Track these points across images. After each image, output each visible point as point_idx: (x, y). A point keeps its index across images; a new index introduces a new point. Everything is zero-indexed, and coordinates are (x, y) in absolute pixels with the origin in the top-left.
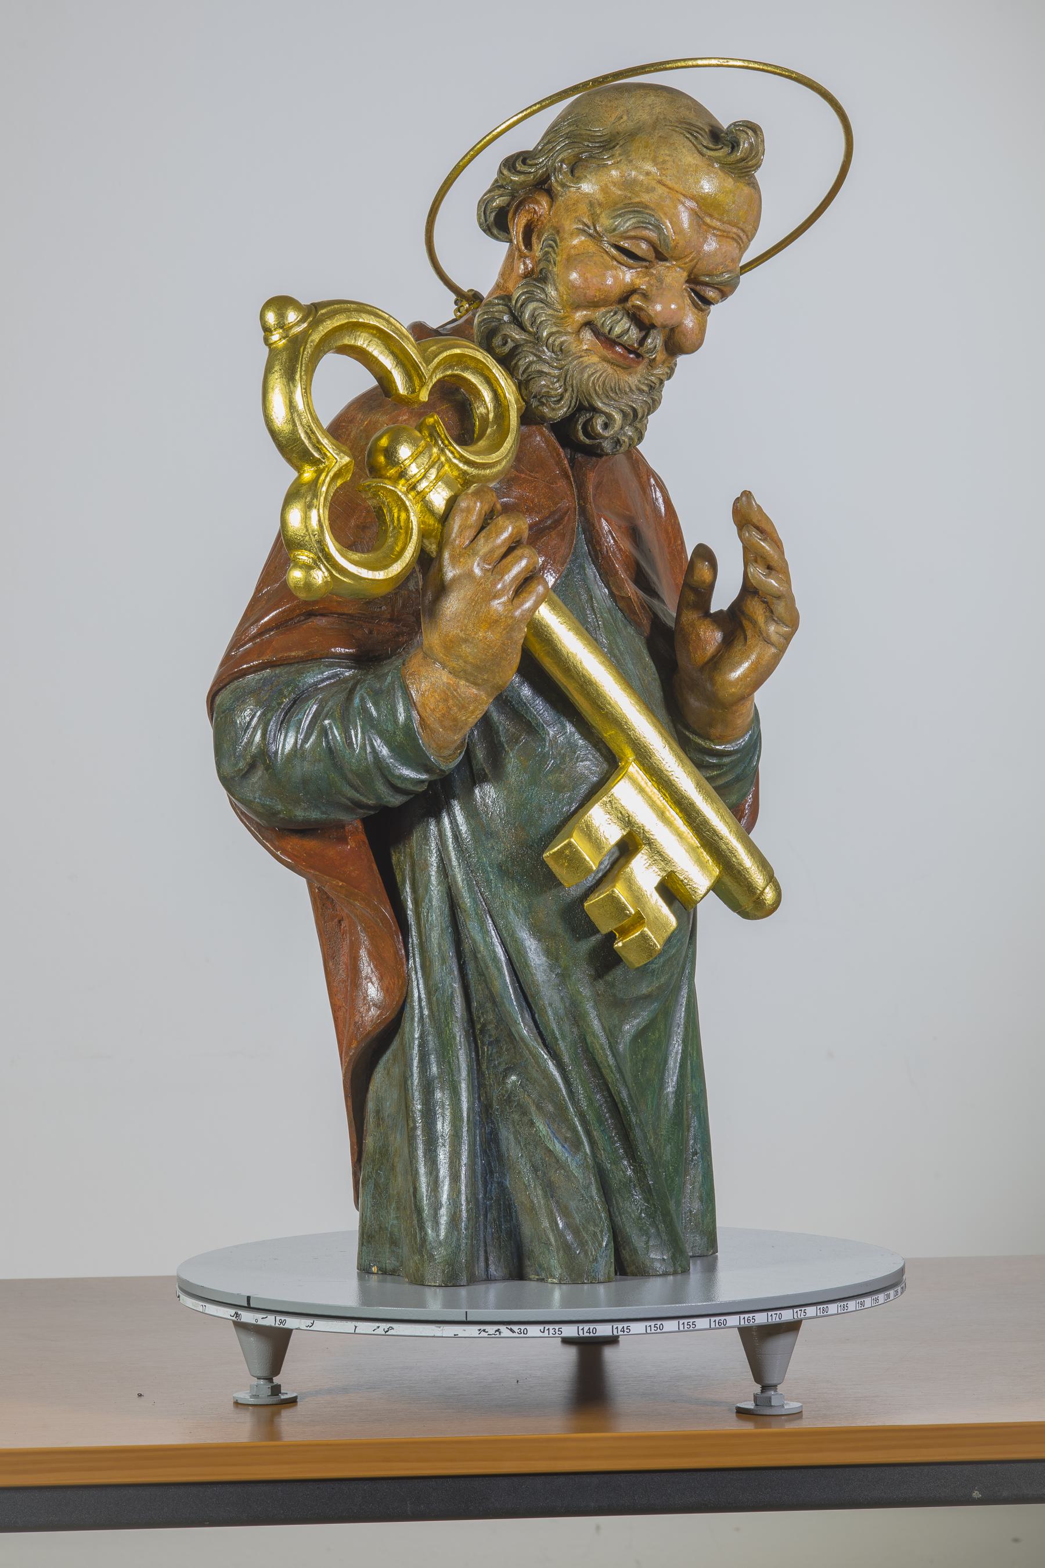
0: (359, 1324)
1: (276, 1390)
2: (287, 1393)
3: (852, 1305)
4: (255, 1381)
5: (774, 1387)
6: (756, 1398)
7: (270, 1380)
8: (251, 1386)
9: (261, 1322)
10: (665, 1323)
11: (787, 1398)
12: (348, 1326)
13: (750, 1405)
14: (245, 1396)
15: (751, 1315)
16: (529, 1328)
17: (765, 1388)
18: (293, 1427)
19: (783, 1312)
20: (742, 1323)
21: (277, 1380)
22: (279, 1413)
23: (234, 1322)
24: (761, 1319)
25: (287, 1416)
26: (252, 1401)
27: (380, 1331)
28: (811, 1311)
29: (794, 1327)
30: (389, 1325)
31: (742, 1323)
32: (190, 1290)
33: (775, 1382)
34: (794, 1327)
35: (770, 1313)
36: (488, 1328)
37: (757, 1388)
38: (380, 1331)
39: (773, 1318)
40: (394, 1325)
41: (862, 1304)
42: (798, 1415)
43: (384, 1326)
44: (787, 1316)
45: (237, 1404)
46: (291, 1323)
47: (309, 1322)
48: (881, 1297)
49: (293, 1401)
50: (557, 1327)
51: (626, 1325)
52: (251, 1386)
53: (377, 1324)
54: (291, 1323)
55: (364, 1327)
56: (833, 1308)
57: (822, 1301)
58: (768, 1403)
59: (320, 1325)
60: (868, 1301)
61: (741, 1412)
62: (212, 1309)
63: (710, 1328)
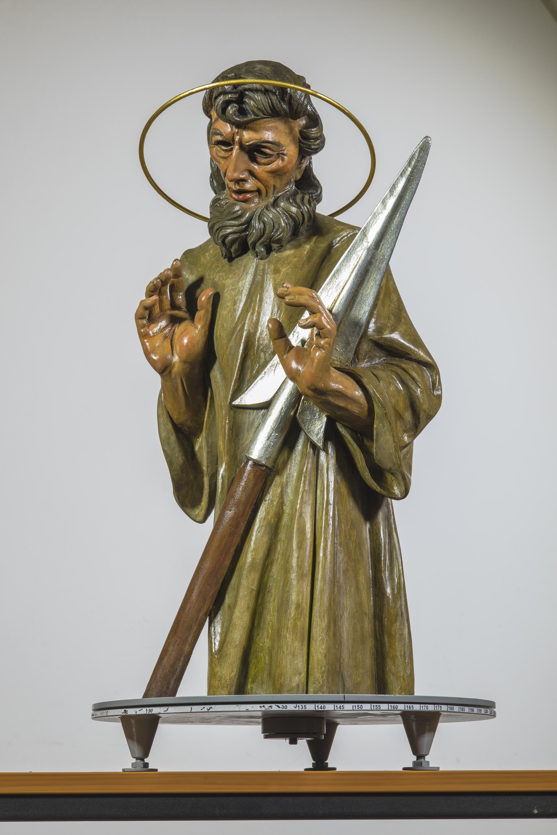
0: (193, 707)
9: (139, 713)
12: (187, 709)
15: (411, 705)
20: (406, 708)
24: (417, 707)
27: (205, 710)
31: (406, 708)
35: (421, 705)
36: (266, 705)
39: (423, 708)
40: (213, 706)
43: (207, 707)
44: (431, 708)
46: (156, 710)
47: (165, 708)
53: (202, 706)
54: (156, 710)
55: (196, 708)
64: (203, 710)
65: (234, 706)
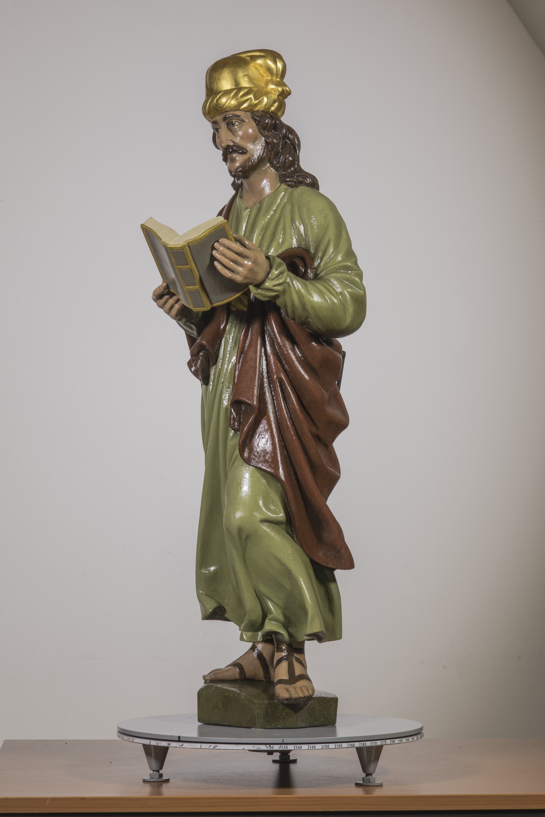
0: (203, 745)
1: (161, 776)
2: (165, 778)
3: (404, 740)
4: (152, 772)
5: (371, 774)
6: (363, 779)
7: (158, 771)
8: (150, 774)
10: (330, 745)
11: (377, 777)
13: (361, 782)
14: (147, 778)
16: (274, 746)
17: (367, 775)
18: (168, 791)
19: (377, 741)
21: (161, 772)
22: (162, 785)
23: (144, 746)
25: (164, 785)
26: (152, 780)
28: (388, 742)
29: (379, 749)
30: (214, 745)
32: (123, 733)
33: (371, 772)
34: (380, 748)
37: (364, 775)
38: (212, 747)
41: (408, 740)
42: (381, 785)
44: (379, 743)
45: (144, 781)
48: (415, 737)
49: (167, 781)
50: (286, 746)
51: (314, 745)
52: (150, 774)
55: (204, 746)
56: (397, 741)
57: (393, 737)
58: (369, 781)
59: (186, 745)
60: (410, 739)
61: (357, 785)
62: (137, 740)
63: (348, 747)
64: (211, 748)
65: (234, 745)
